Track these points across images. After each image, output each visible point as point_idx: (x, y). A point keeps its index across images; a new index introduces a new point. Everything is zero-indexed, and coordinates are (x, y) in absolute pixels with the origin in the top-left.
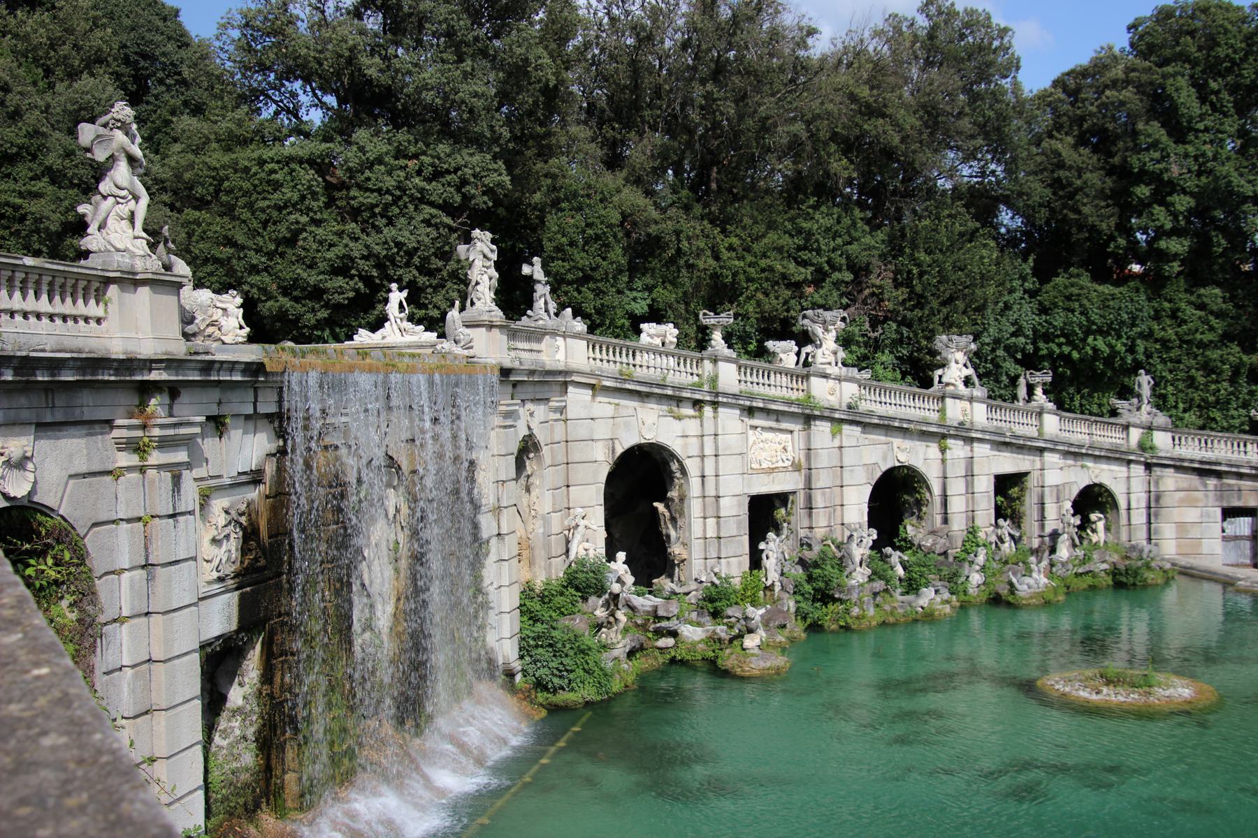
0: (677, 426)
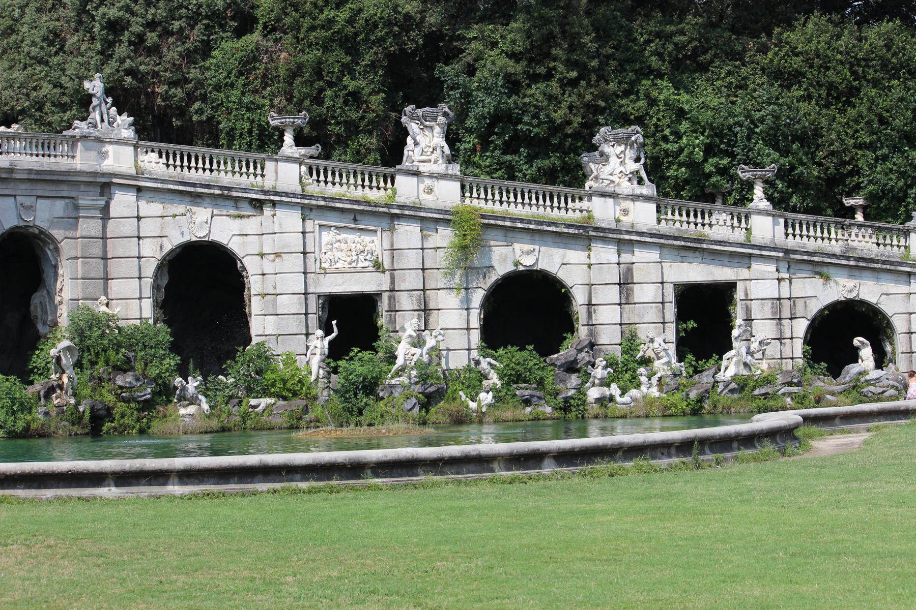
0: (236, 225)
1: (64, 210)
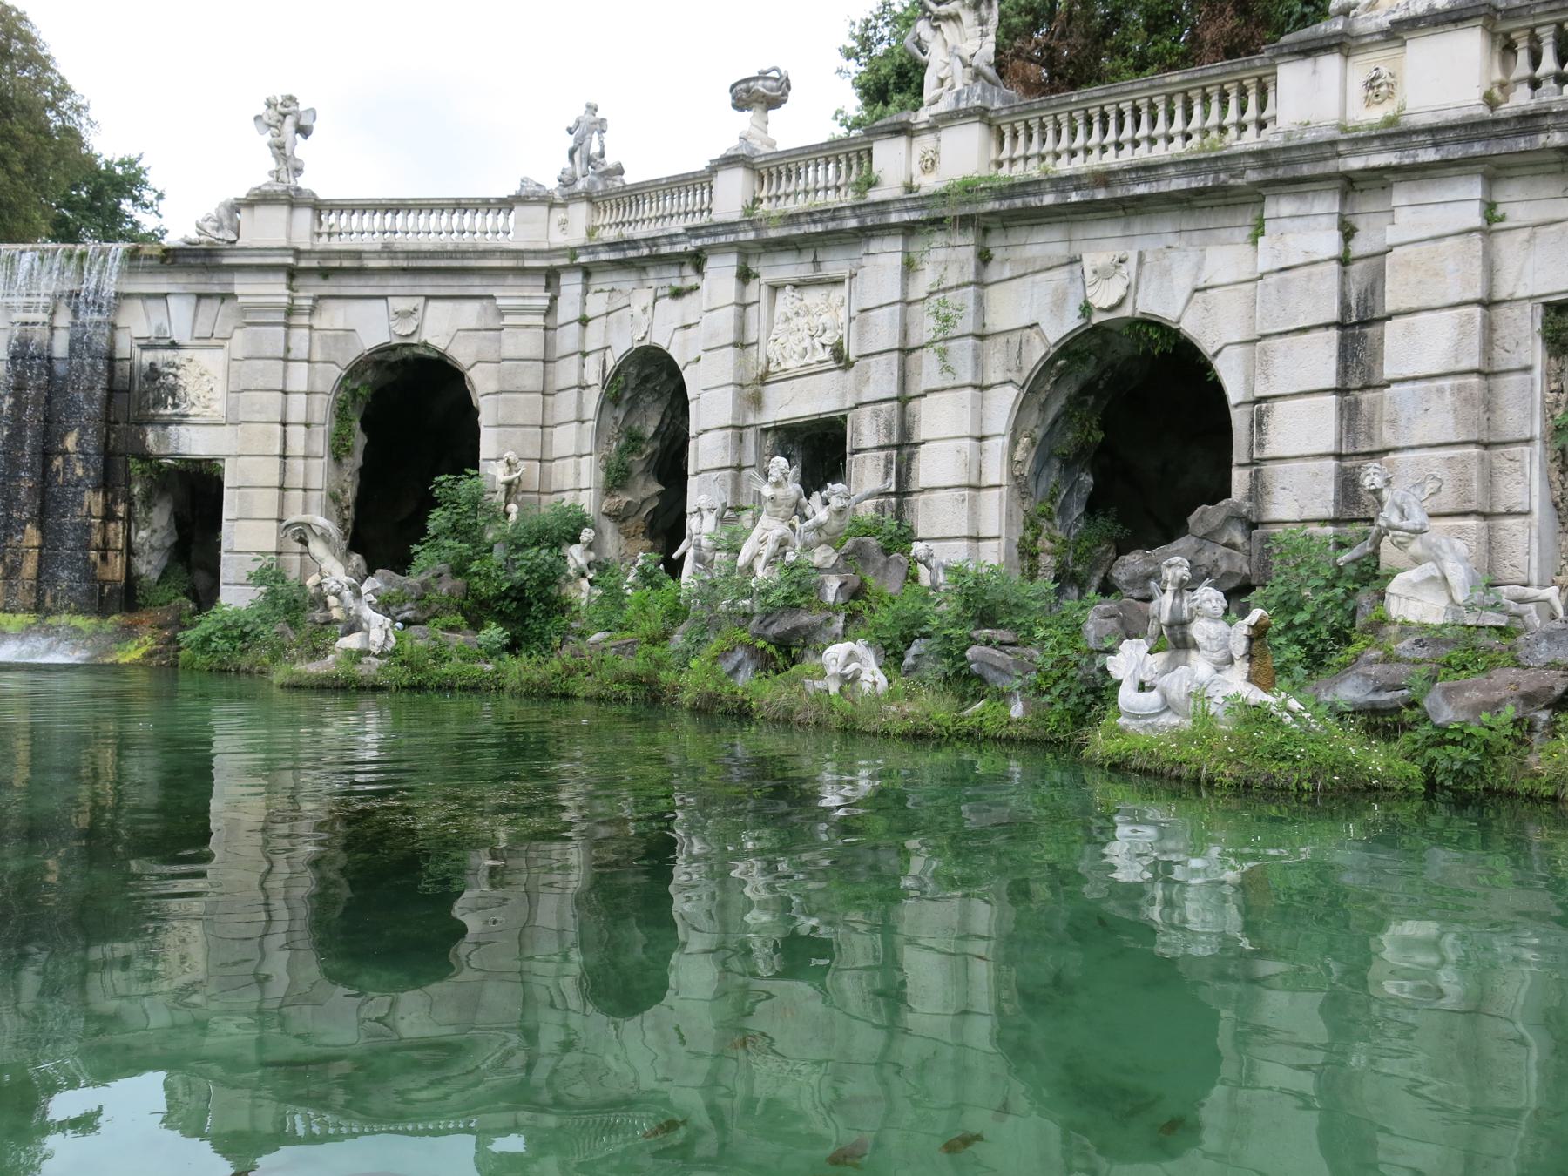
1: (479, 318)
